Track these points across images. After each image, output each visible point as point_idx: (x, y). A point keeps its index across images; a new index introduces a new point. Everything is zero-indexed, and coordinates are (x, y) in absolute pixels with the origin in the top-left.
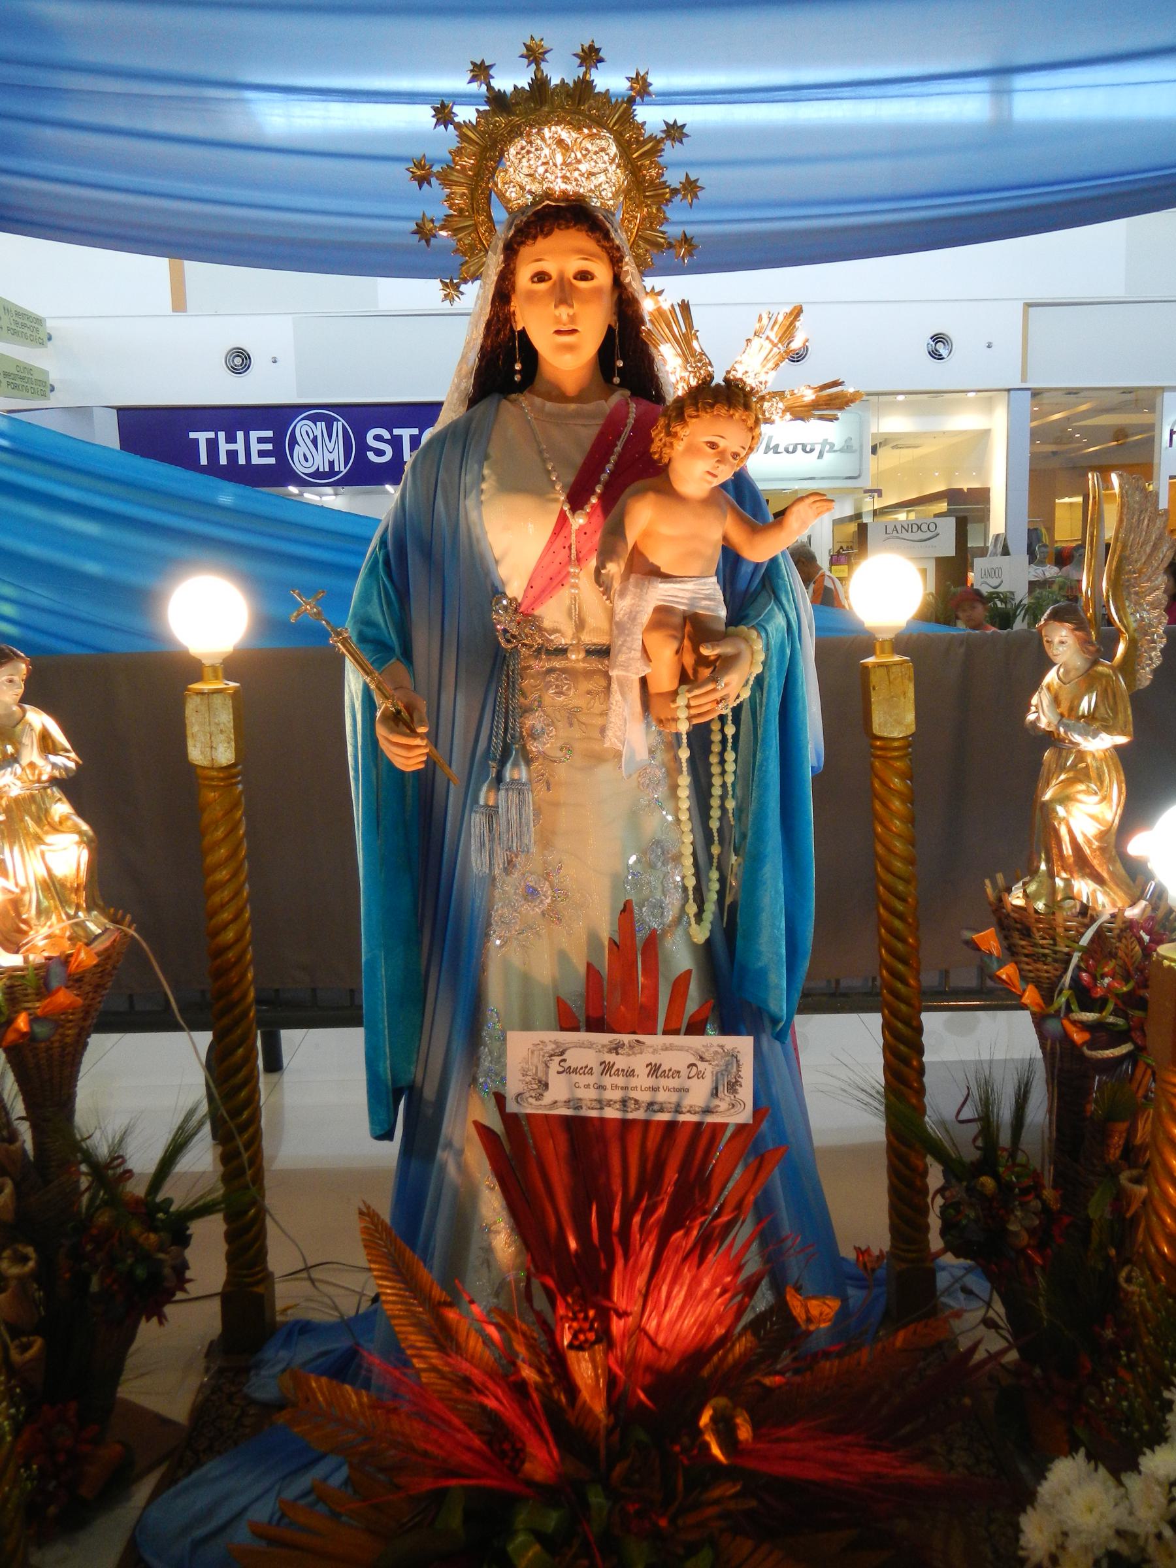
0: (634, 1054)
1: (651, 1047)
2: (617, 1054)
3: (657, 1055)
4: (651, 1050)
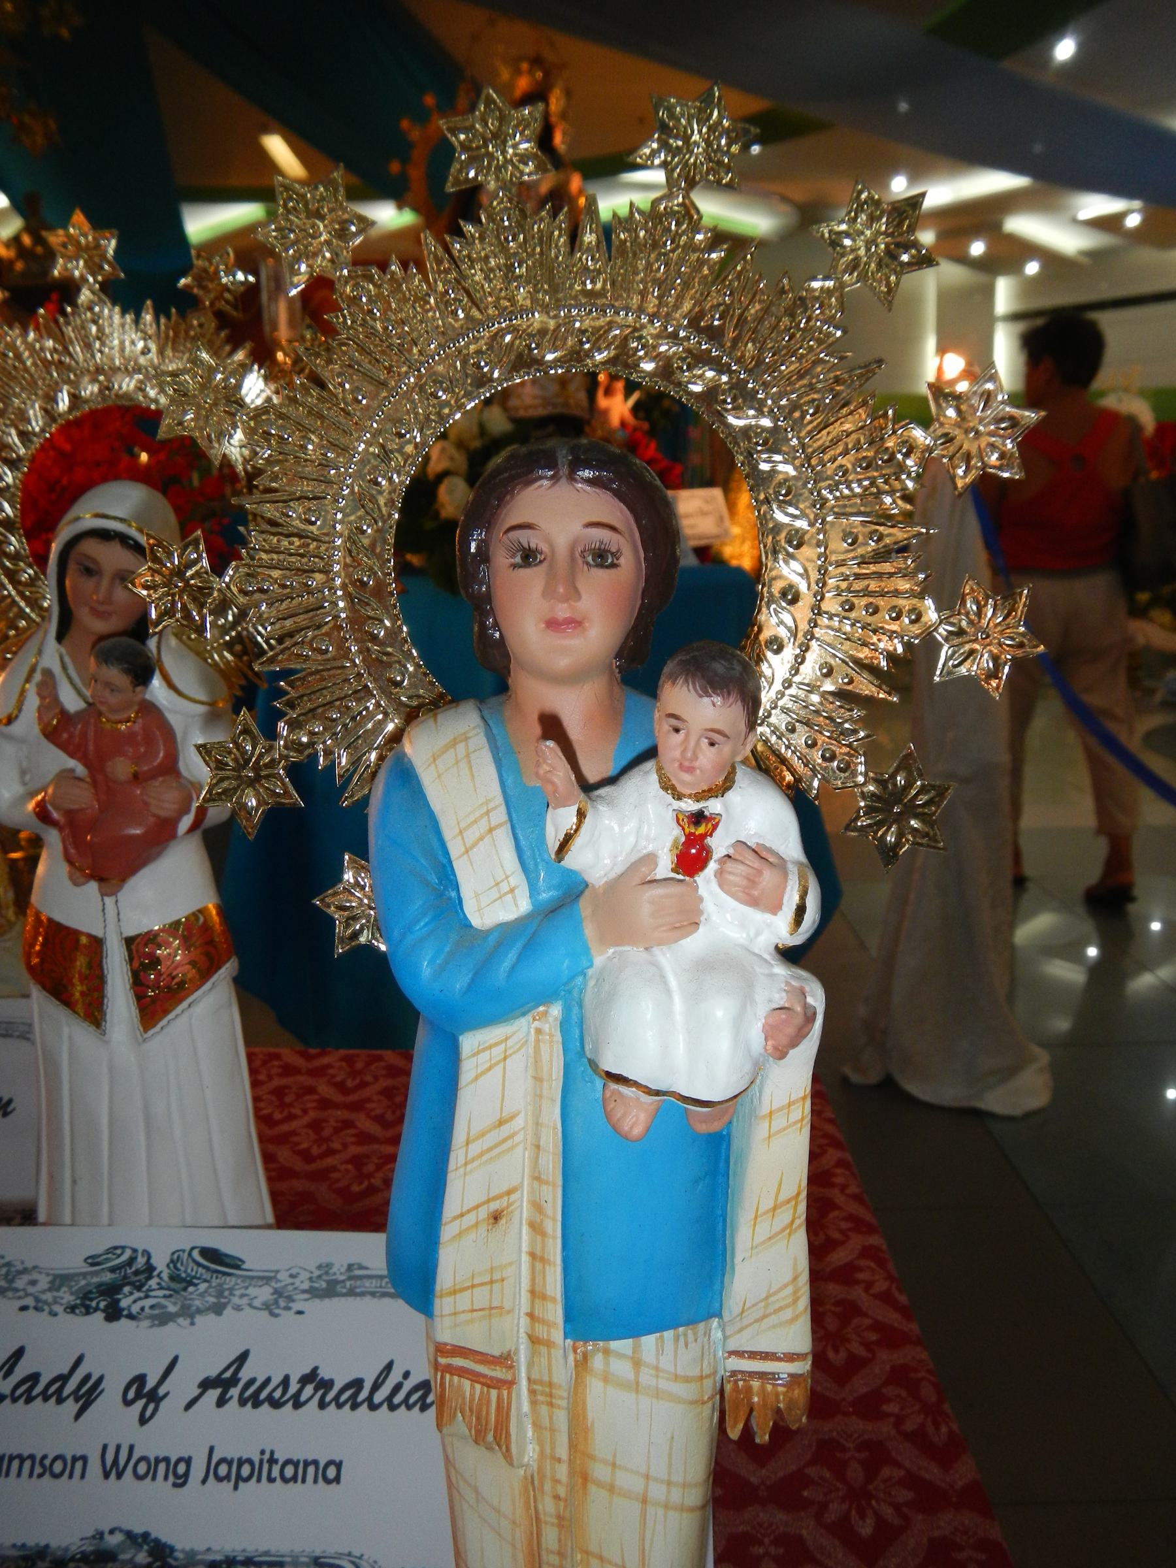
0: (188, 1313)
1: (267, 1279)
2: (114, 1313)
3: (288, 1317)
4: (264, 1294)
